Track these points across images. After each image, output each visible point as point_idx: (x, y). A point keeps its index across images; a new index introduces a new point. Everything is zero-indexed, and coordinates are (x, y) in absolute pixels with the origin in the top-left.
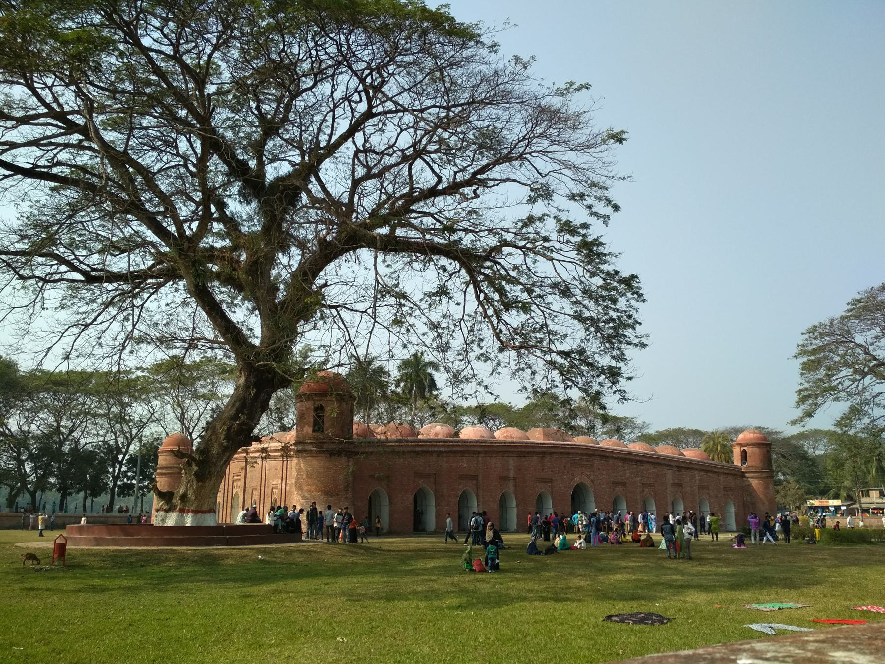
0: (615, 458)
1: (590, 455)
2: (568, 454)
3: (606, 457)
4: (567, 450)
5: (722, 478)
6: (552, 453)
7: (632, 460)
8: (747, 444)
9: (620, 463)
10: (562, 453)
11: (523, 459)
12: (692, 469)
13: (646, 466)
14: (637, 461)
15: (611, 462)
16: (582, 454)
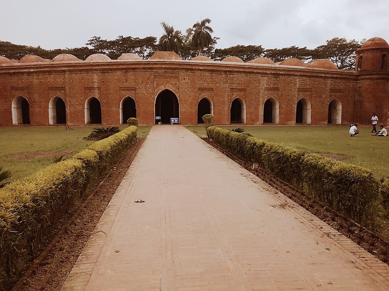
0: (201, 70)
1: (175, 69)
2: (151, 69)
3: (192, 69)
4: (151, 66)
5: (329, 82)
6: (134, 69)
7: (220, 71)
8: (363, 51)
9: (207, 74)
10: (144, 68)
11: (106, 74)
12: (291, 75)
13: (236, 75)
14: (226, 72)
15: (198, 73)
16: (165, 68)
